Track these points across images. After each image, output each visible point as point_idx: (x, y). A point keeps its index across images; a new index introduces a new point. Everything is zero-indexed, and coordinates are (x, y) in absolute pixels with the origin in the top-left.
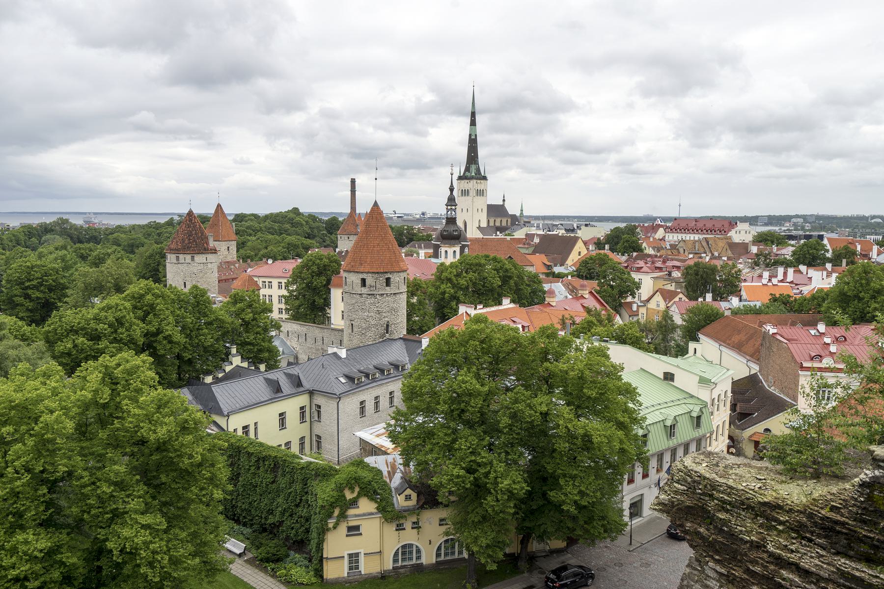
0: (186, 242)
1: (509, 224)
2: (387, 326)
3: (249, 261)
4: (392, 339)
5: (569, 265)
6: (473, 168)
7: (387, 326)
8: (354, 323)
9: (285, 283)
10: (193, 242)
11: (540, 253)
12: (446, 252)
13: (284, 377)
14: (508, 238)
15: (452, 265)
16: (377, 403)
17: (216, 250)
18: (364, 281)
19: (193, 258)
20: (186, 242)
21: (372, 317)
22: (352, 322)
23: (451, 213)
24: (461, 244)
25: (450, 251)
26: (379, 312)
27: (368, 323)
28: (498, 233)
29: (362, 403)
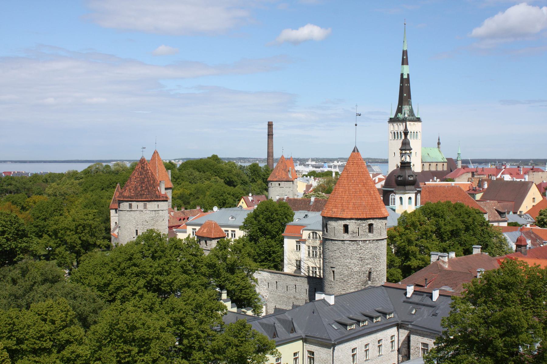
0: (139, 189)
1: (445, 169)
2: (370, 273)
3: (183, 210)
4: (374, 287)
5: (523, 213)
6: (406, 109)
7: (370, 273)
8: (335, 269)
9: (232, 231)
10: (145, 189)
11: (490, 200)
12: (401, 198)
13: (276, 322)
14: (453, 183)
15: (414, 213)
16: (366, 351)
17: (167, 198)
18: (346, 228)
19: (145, 207)
20: (139, 189)
21: (355, 264)
22: (333, 269)
23: (406, 158)
24: (416, 190)
25: (405, 197)
26: (361, 259)
27: (350, 270)
28: (435, 178)
29: (353, 350)
